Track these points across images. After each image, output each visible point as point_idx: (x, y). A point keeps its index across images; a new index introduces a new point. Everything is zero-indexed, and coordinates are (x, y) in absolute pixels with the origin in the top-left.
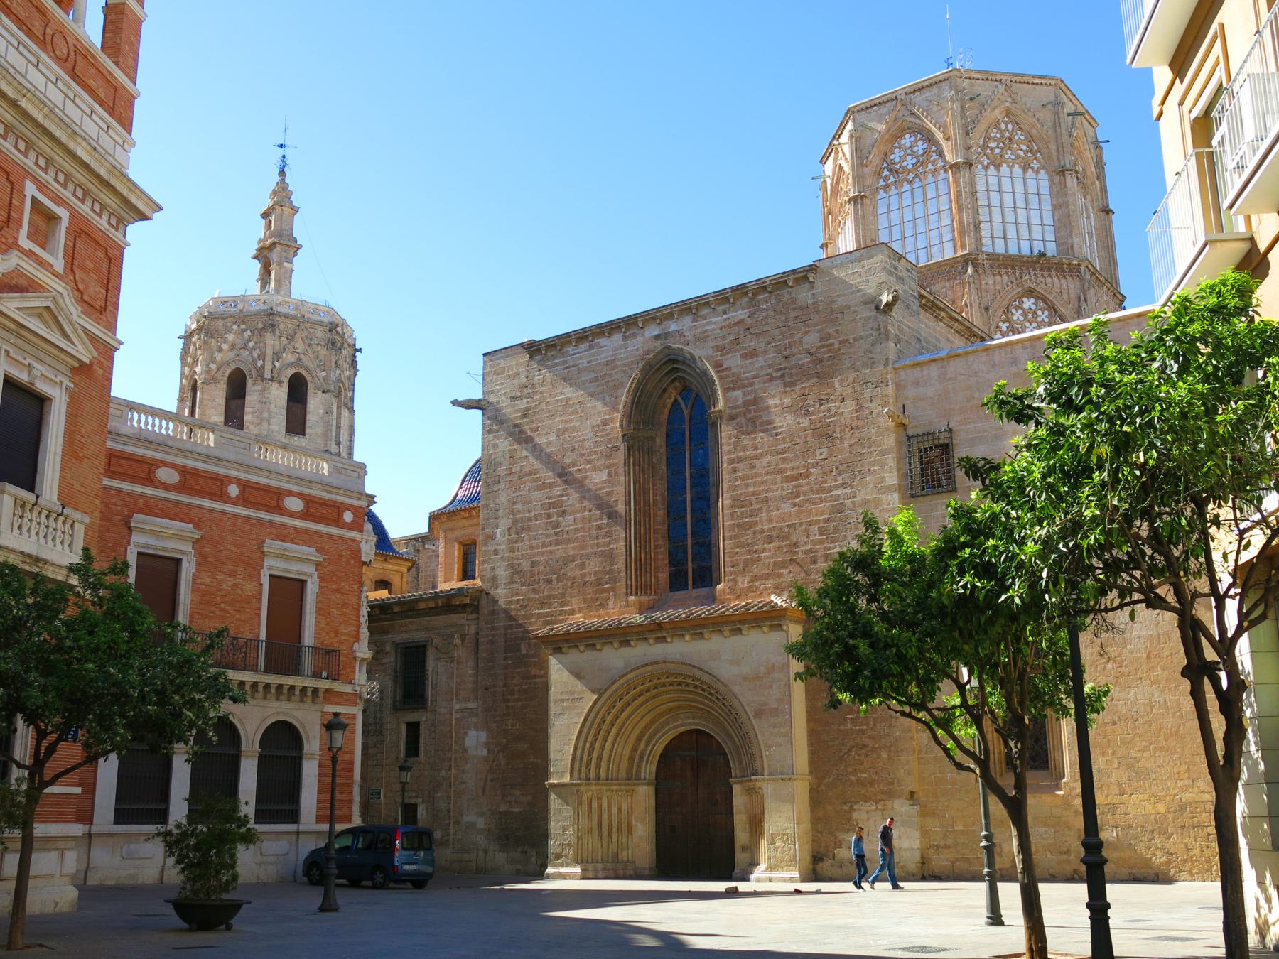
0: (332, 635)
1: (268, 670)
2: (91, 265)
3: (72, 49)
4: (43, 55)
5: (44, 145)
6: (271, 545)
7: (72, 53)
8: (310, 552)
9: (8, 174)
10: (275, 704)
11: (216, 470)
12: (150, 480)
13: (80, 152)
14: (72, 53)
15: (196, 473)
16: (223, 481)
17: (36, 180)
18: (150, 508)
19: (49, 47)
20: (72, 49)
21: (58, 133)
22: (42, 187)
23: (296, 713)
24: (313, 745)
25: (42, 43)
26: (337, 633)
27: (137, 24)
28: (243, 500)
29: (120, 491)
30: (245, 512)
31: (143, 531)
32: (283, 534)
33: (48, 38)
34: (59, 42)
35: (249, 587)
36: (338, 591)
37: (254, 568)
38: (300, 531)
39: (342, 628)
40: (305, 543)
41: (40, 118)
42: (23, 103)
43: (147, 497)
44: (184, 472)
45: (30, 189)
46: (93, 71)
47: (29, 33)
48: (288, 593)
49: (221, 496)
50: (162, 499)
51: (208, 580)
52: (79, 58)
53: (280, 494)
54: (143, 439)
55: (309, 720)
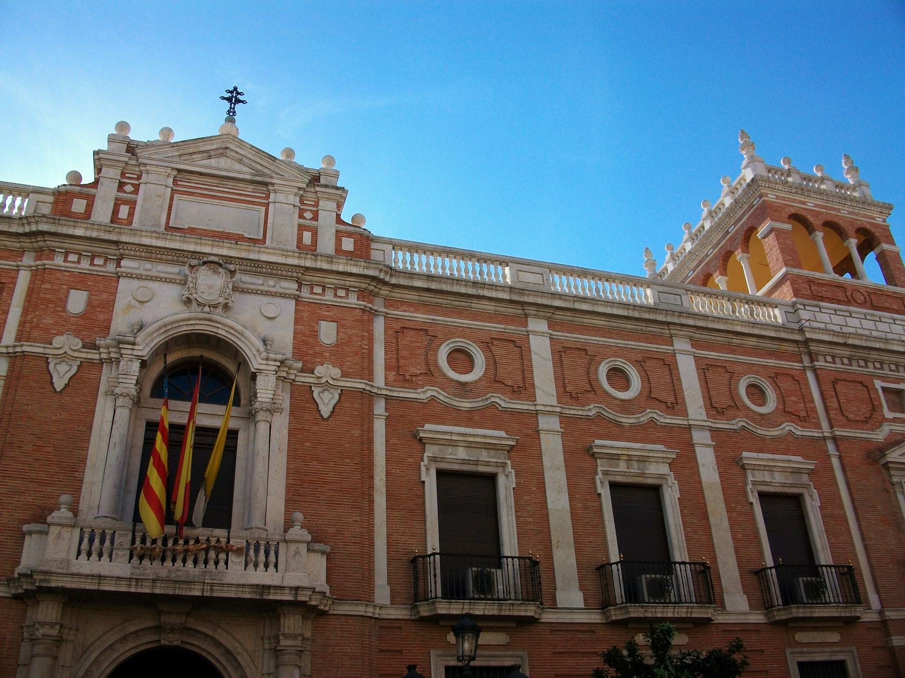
3: (865, 294)
4: (851, 308)
5: (874, 355)
7: (867, 296)
9: (861, 383)
13: (896, 348)
14: (867, 296)
17: (879, 377)
19: (853, 302)
20: (865, 294)
21: (877, 345)
22: (884, 378)
25: (848, 302)
27: (897, 256)
33: (850, 297)
34: (857, 296)
41: (864, 344)
42: (850, 342)
45: (878, 384)
46: (884, 298)
47: (839, 302)
52: (872, 296)
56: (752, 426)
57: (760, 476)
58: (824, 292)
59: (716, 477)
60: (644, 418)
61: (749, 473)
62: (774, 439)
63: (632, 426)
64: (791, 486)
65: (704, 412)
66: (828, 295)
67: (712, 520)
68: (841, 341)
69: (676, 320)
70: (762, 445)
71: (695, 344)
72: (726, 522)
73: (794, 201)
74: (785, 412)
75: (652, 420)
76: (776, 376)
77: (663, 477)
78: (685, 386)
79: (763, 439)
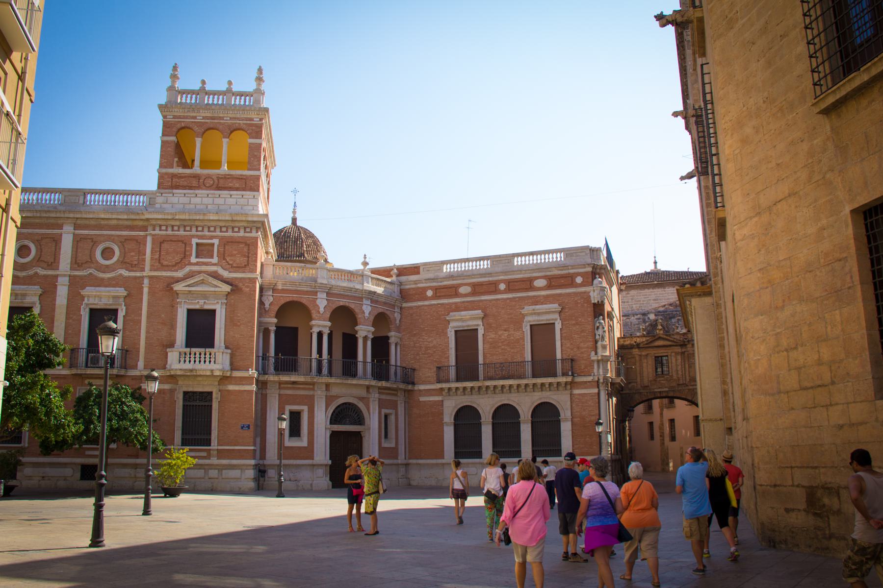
0: (575, 350)
1: (534, 376)
2: (235, 252)
6: (528, 309)
8: (555, 306)
10: (540, 393)
11: (491, 279)
12: (457, 295)
15: (481, 284)
16: (495, 284)
18: (457, 308)
23: (555, 397)
24: (565, 414)
26: (578, 348)
28: (509, 290)
29: (442, 304)
30: (510, 296)
31: (453, 320)
32: (536, 301)
35: (518, 334)
36: (577, 324)
37: (518, 323)
38: (547, 296)
39: (582, 345)
40: (551, 303)
43: (456, 303)
44: (474, 286)
48: (542, 333)
49: (496, 291)
50: (464, 302)
51: (493, 336)
53: (531, 280)
54: (451, 276)
55: (561, 400)
56: (96, 273)
57: (92, 301)
58: (182, 182)
59: (65, 302)
60: (31, 272)
61: (86, 299)
62: (109, 279)
63: (24, 277)
64: (111, 305)
65: (69, 266)
66: (185, 183)
67: (56, 324)
68: (170, 217)
69: (62, 215)
70: (100, 283)
71: (77, 227)
72: (63, 325)
73: (187, 117)
74: (124, 263)
75: (36, 273)
76: (123, 242)
77: (34, 303)
78: (62, 251)
79: (102, 279)
